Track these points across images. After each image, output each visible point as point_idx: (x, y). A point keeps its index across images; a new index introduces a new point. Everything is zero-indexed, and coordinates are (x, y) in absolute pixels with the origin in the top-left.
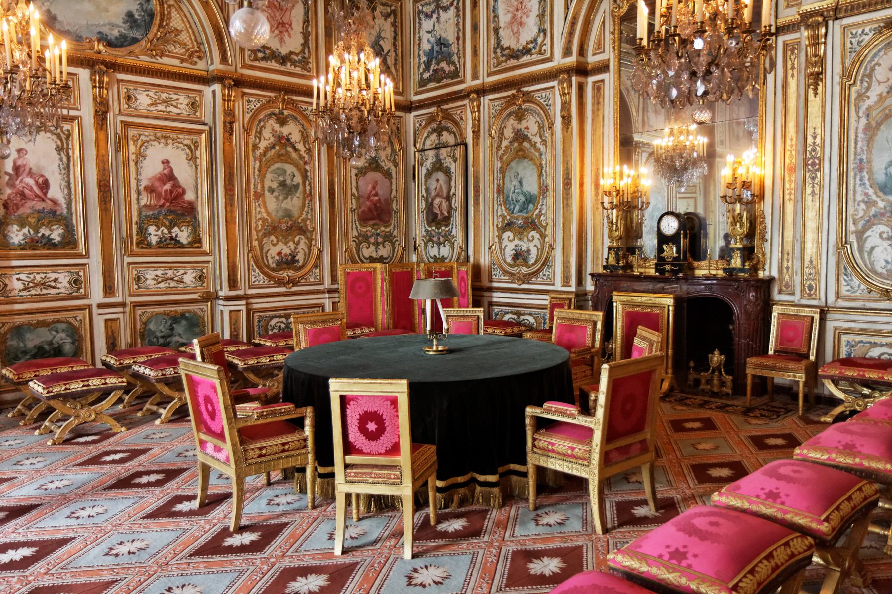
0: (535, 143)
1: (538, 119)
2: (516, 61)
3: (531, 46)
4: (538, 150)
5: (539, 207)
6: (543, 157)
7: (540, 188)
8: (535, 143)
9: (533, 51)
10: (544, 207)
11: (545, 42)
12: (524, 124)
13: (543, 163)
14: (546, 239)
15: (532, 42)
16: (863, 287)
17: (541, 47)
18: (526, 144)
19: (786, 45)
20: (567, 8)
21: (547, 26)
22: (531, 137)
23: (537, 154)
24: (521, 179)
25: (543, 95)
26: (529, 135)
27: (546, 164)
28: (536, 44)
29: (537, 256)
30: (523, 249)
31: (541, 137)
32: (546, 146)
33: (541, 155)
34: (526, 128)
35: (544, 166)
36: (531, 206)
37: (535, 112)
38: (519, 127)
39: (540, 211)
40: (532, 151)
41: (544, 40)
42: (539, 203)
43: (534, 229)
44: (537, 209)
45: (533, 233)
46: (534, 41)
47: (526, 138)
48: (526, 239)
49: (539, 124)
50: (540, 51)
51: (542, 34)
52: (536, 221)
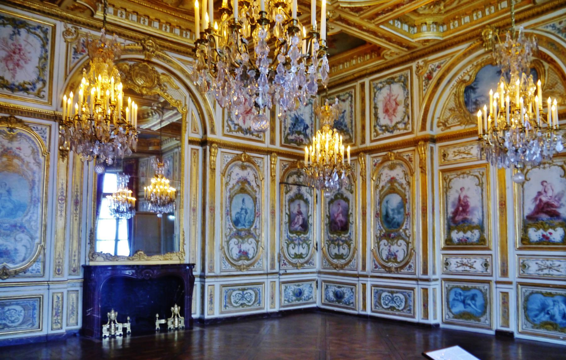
0: (28, 163)
1: (33, 145)
2: (10, 92)
3: (29, 87)
4: (31, 170)
5: (29, 215)
6: (36, 175)
7: (31, 200)
8: (28, 163)
9: (31, 91)
10: (35, 215)
11: (44, 89)
12: (15, 145)
13: (37, 180)
14: (37, 241)
15: (30, 84)
16: (229, 265)
17: (40, 91)
18: (16, 161)
19: (198, 150)
20: (66, 75)
21: (47, 78)
22: (23, 157)
23: (30, 173)
24: (10, 189)
25: (39, 128)
26: (21, 155)
27: (39, 181)
28: (35, 87)
29: (26, 254)
30: (9, 248)
31: (35, 159)
32: (40, 168)
33: (34, 173)
34: (17, 148)
35: (37, 182)
36: (20, 213)
37: (29, 138)
38: (9, 145)
39: (30, 218)
40: (24, 167)
41: (43, 88)
42: (29, 211)
43: (23, 232)
44: (27, 215)
45: (22, 235)
46: (34, 84)
47: (17, 156)
48: (13, 241)
49: (33, 150)
50: (38, 94)
51: (41, 83)
52: (27, 225)
